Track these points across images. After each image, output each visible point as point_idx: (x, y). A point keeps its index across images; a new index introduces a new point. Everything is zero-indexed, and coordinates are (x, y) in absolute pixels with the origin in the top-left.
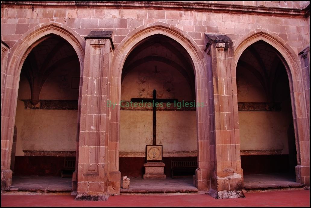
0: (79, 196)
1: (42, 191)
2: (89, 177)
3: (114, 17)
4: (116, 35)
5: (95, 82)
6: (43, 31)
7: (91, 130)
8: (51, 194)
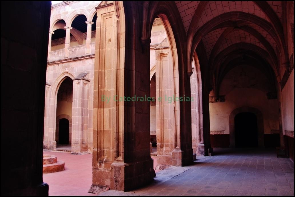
0: (72, 152)
1: (65, 151)
2: (76, 144)
3: (90, 64)
4: (91, 74)
5: (78, 101)
6: (63, 75)
7: (76, 123)
8: (68, 152)
